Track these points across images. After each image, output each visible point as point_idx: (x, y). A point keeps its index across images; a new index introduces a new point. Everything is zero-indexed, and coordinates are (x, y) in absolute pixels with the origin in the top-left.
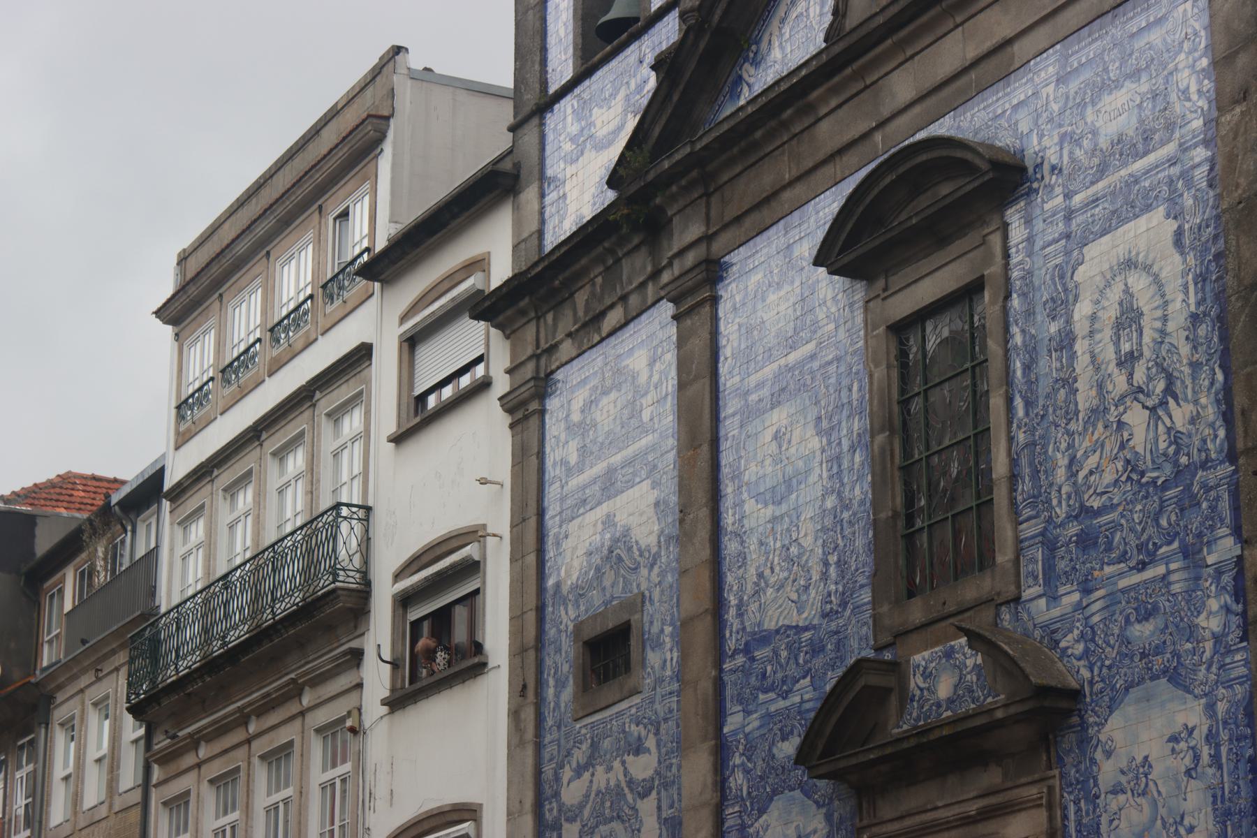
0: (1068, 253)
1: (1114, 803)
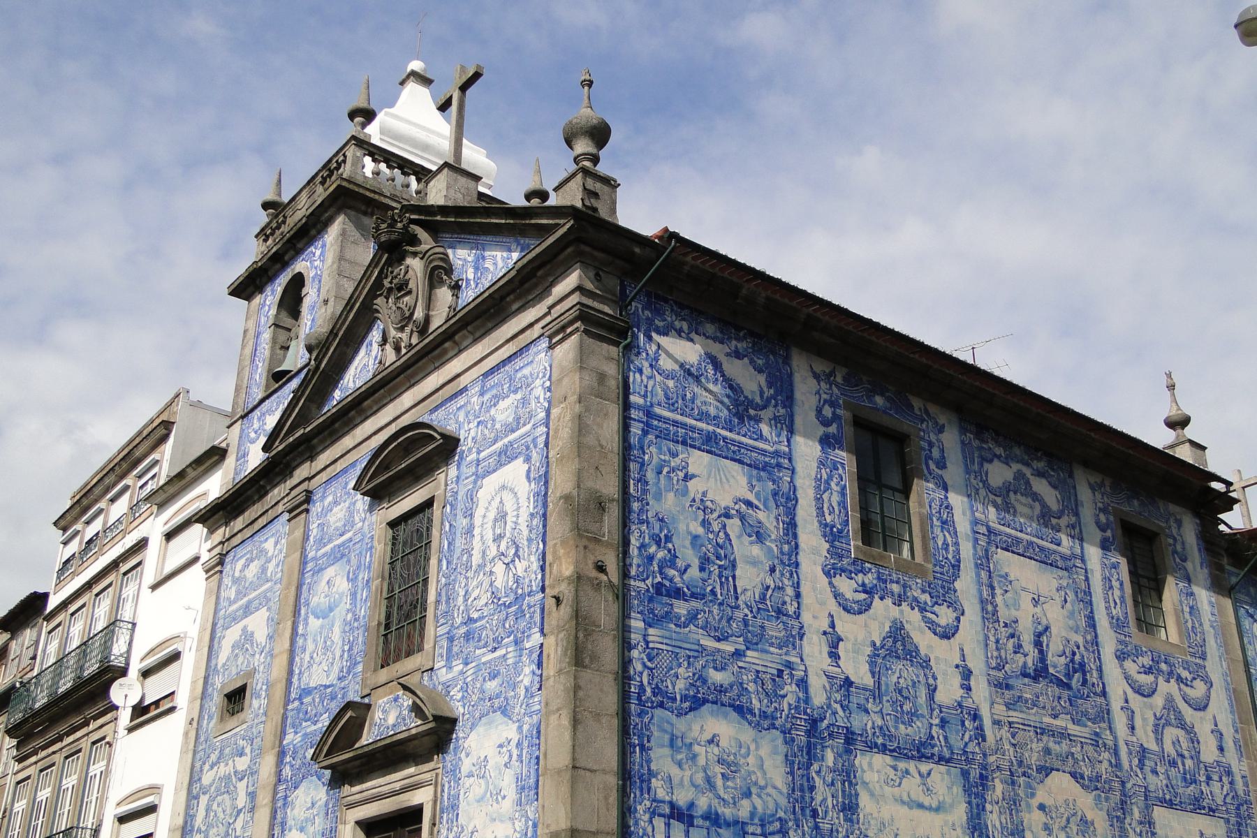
0: (475, 482)
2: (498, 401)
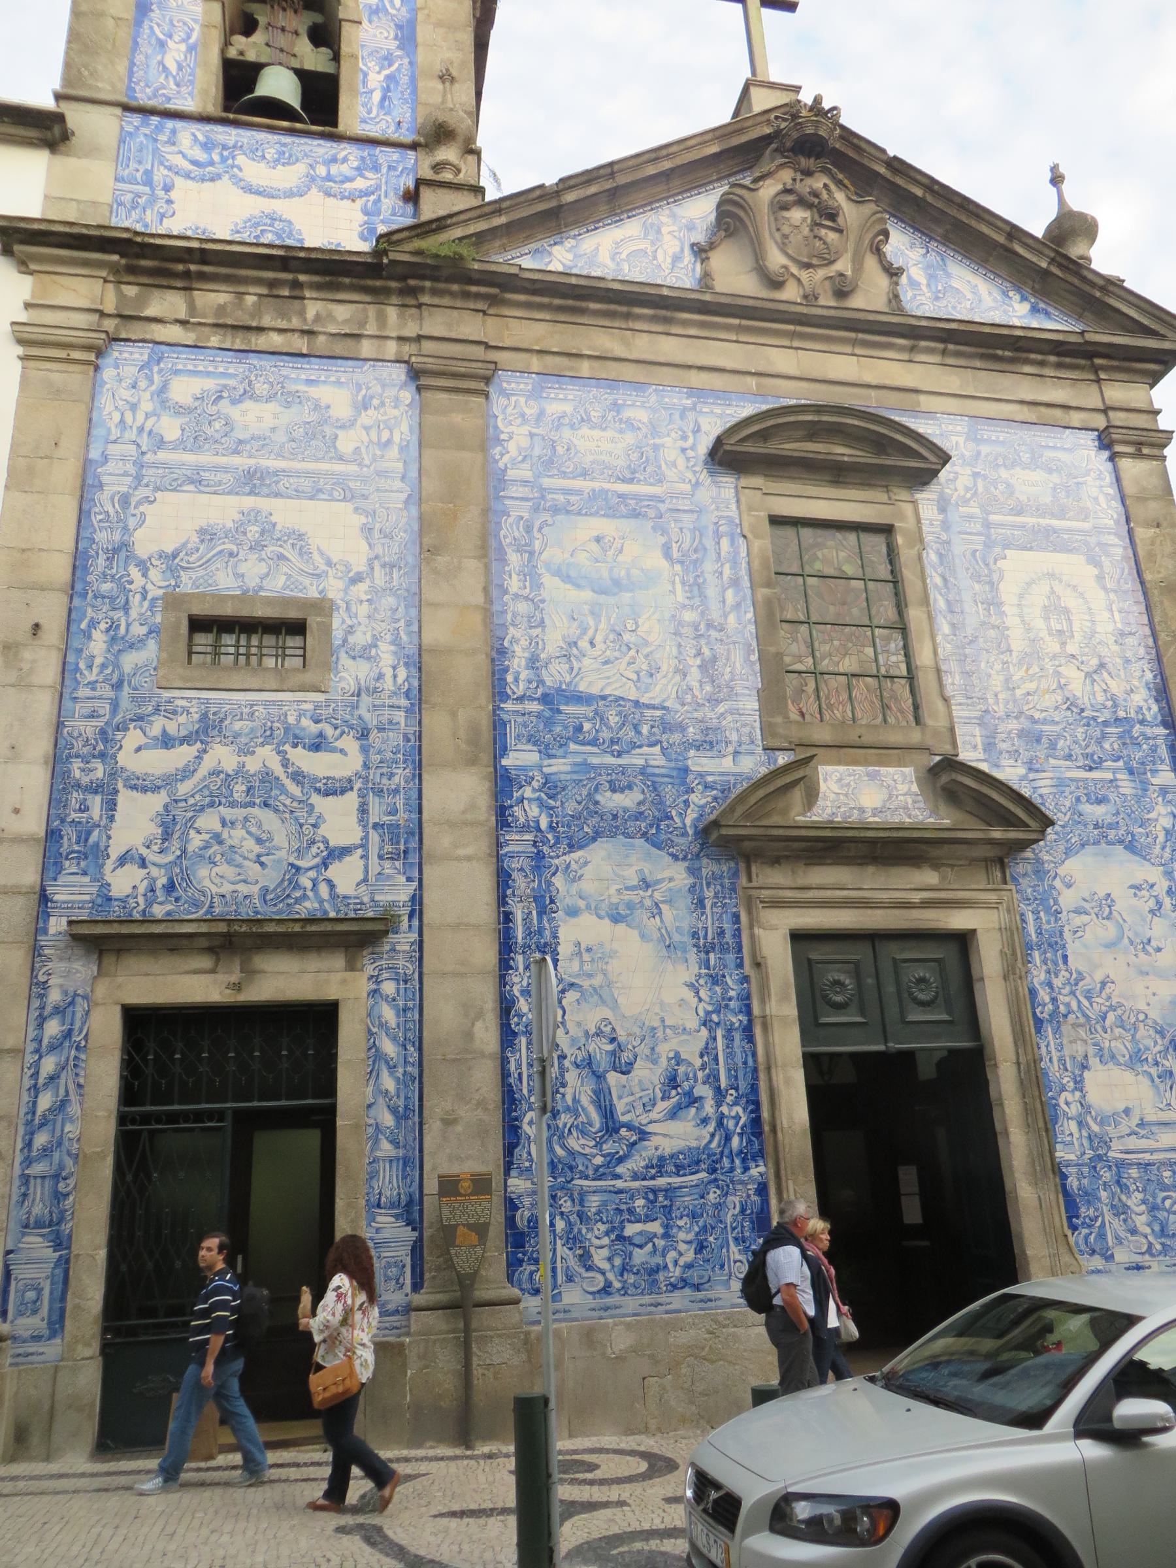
0: (988, 545)
1: (1078, 920)
2: (1013, 465)
